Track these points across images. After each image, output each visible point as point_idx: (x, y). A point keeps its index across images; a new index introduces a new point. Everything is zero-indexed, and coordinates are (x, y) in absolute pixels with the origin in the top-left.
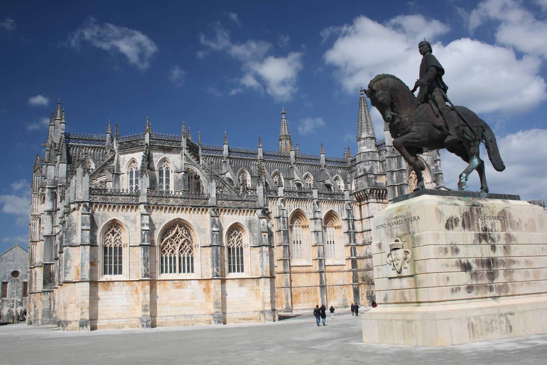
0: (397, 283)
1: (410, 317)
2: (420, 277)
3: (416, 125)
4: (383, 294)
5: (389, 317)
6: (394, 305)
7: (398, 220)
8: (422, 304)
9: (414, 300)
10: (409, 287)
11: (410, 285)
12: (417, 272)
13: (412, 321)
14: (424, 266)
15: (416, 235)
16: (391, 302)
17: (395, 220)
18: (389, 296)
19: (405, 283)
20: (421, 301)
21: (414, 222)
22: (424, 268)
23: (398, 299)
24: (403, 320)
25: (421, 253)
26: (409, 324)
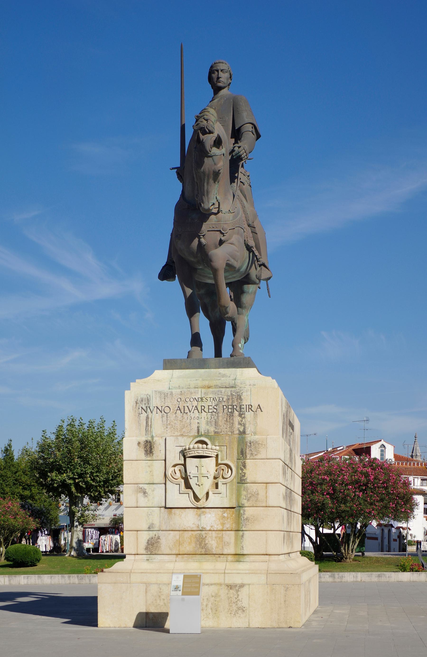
0: (189, 519)
1: (238, 580)
2: (249, 512)
3: (238, 233)
4: (144, 537)
6: (173, 557)
7: (206, 404)
8: (247, 558)
9: (232, 551)
10: (220, 527)
11: (223, 524)
12: (244, 502)
13: (242, 586)
14: (262, 493)
15: (249, 438)
16: (168, 551)
19: (210, 519)
20: (245, 552)
24: (221, 585)
25: (255, 470)
26: (231, 591)
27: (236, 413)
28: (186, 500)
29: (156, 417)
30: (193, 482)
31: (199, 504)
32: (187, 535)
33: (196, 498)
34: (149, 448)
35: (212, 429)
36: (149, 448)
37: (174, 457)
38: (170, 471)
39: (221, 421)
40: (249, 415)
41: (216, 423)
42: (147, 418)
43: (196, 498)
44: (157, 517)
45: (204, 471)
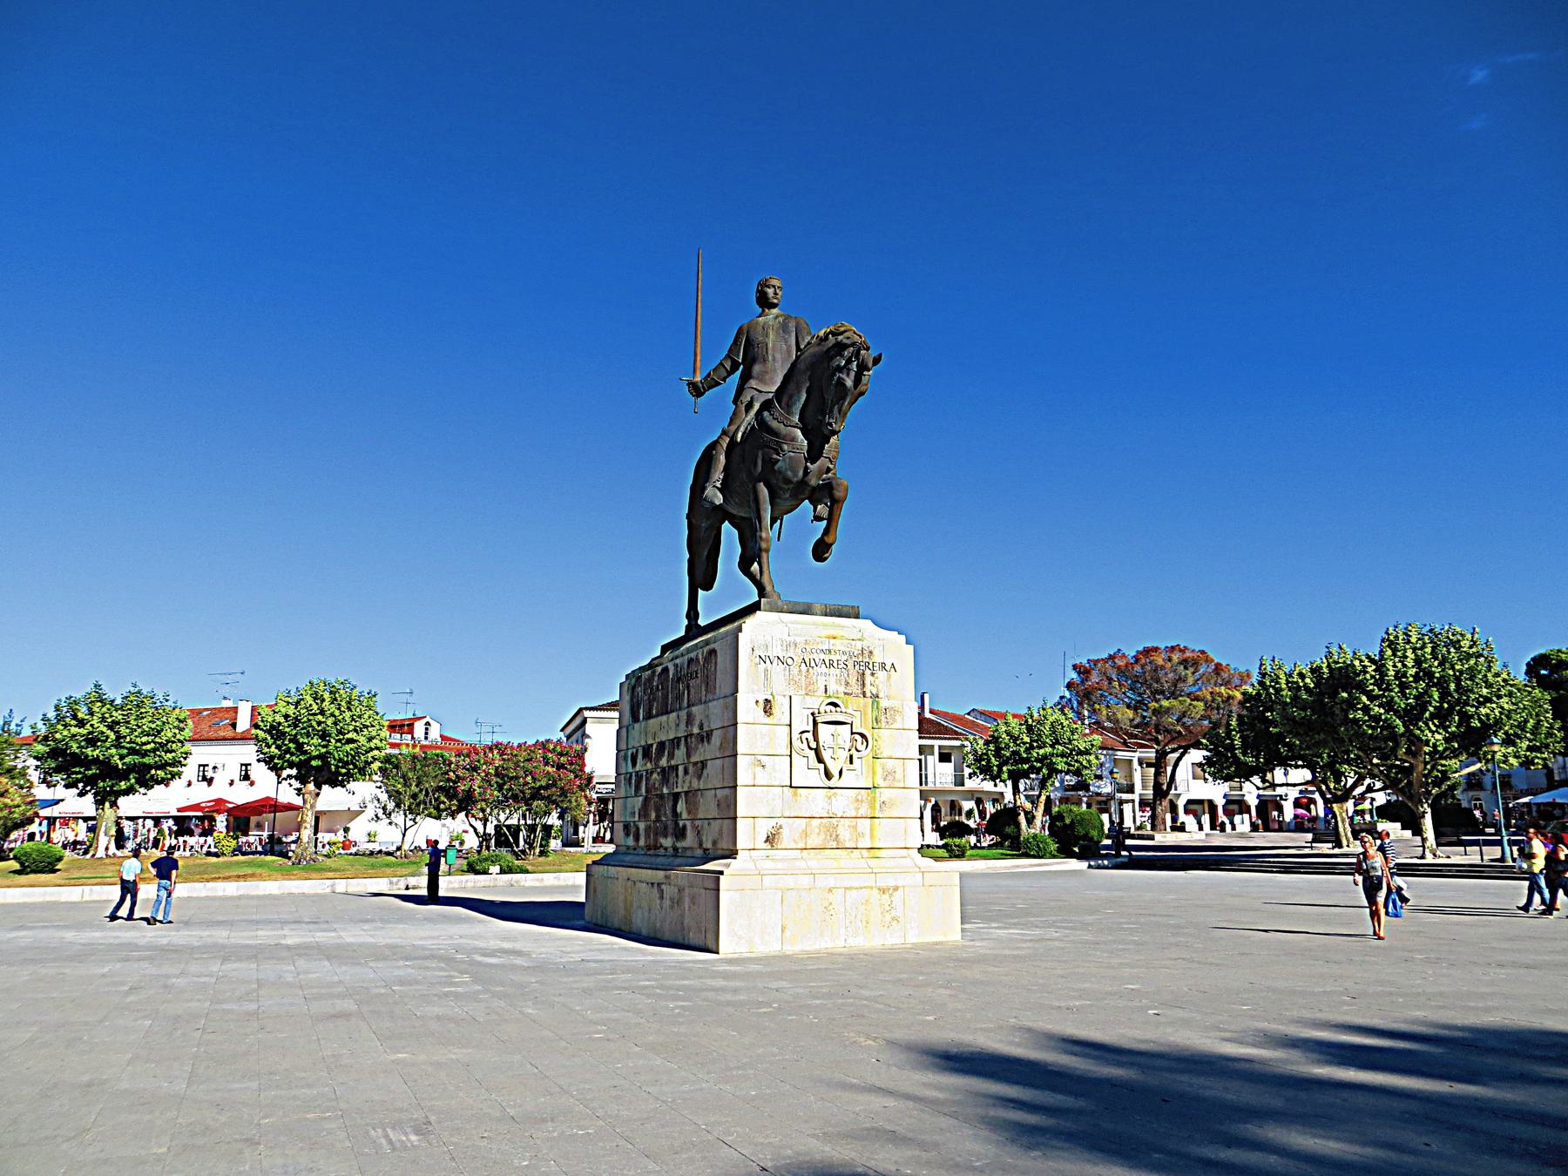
0: (817, 802)
4: (764, 828)
5: (831, 882)
17: (822, 656)
18: (785, 832)
19: (842, 802)
21: (881, 674)
22: (899, 776)
23: (815, 841)
27: (868, 672)
28: (817, 778)
29: (778, 668)
30: (826, 755)
31: (832, 783)
32: (815, 822)
33: (828, 775)
34: (768, 707)
35: (842, 689)
36: (768, 707)
37: (802, 723)
38: (795, 736)
39: (853, 680)
40: (881, 674)
41: (847, 684)
42: (766, 670)
43: (828, 775)
44: (777, 800)
45: (840, 742)
